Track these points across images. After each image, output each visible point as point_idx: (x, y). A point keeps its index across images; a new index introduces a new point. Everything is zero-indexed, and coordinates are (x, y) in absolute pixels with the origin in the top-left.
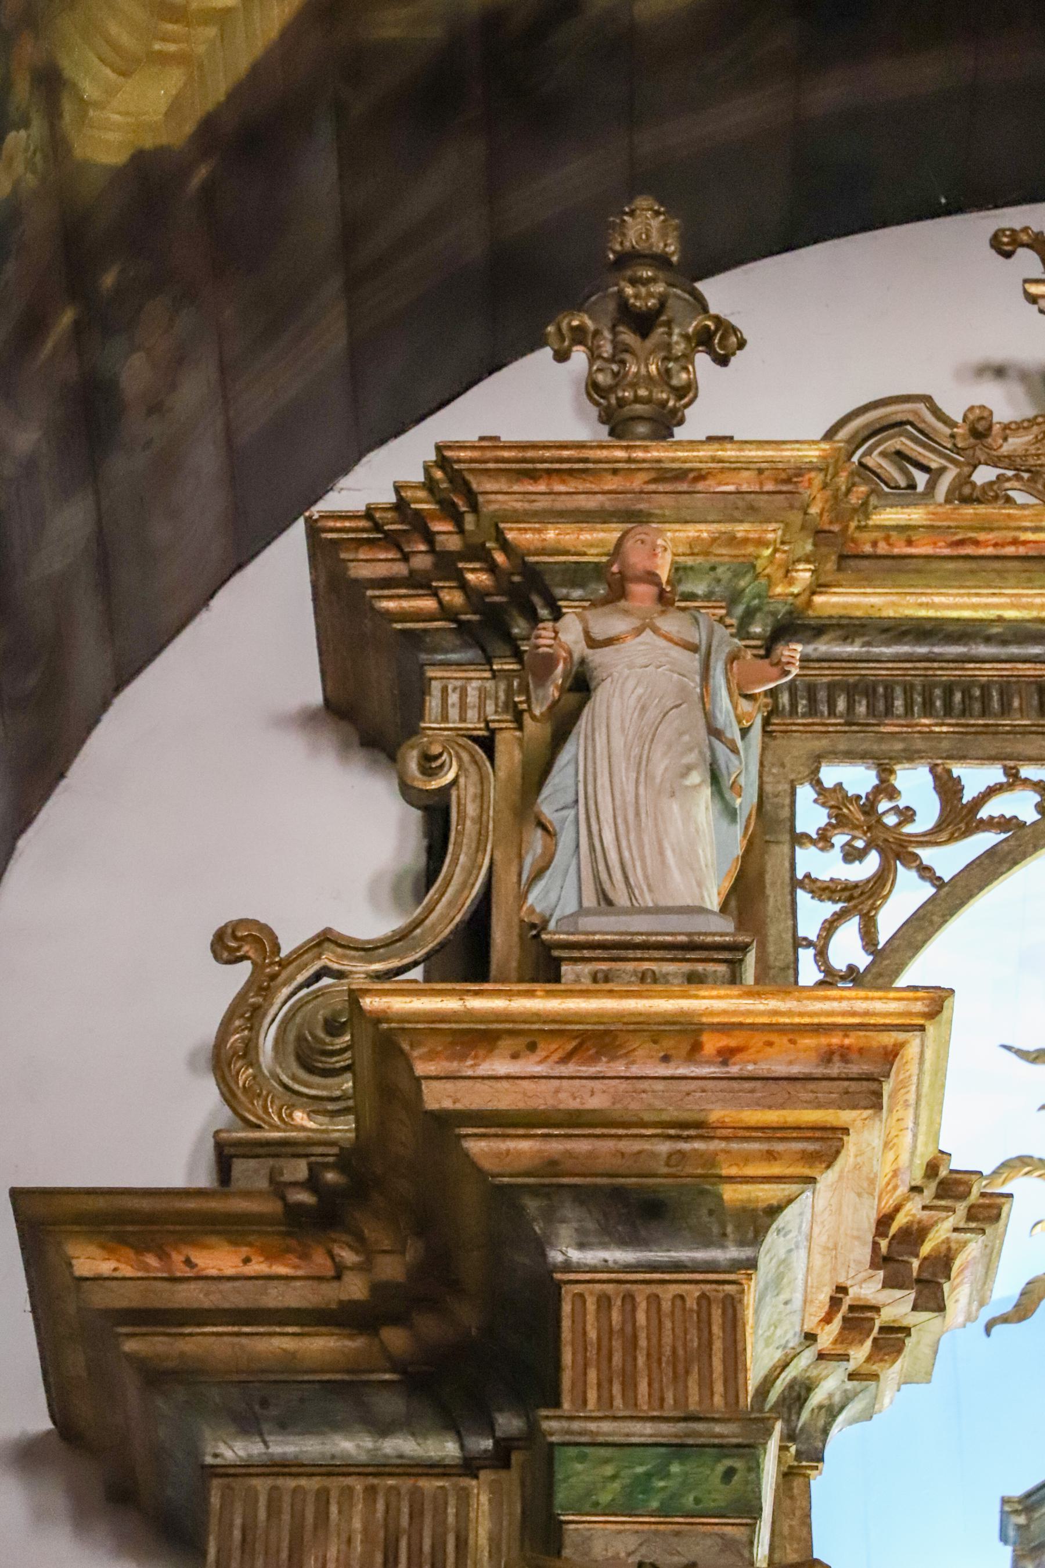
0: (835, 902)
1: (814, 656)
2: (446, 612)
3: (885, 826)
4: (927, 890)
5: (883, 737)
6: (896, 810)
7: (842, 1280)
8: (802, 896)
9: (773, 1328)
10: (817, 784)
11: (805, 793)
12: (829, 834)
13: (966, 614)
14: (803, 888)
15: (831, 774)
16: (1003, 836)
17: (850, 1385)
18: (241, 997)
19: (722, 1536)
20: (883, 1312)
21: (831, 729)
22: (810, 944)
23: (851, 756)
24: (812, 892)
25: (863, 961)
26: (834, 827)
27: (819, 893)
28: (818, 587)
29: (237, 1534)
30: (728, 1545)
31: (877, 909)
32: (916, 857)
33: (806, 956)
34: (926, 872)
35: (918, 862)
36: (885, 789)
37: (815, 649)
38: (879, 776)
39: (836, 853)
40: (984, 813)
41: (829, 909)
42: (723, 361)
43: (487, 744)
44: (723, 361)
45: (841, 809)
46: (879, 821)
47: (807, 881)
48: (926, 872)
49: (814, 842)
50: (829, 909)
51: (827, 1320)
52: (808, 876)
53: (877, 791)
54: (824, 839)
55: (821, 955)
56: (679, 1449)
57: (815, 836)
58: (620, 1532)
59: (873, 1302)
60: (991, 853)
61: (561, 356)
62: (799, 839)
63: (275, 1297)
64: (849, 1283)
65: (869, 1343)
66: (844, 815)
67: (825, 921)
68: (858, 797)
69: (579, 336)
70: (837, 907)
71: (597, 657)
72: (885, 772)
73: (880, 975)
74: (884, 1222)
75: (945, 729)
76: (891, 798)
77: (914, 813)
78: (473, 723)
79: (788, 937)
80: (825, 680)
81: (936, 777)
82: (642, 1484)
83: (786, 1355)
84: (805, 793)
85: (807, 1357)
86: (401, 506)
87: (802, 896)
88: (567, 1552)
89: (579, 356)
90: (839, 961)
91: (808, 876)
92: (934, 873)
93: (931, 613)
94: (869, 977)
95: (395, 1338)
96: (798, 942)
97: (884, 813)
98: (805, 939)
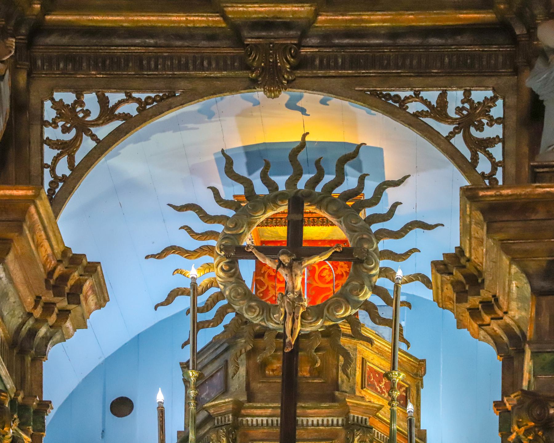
0: (58, 149)
3: (78, 117)
4: (94, 144)
8: (46, 147)
10: (52, 99)
11: (48, 104)
12: (57, 121)
14: (46, 144)
15: (57, 96)
22: (48, 166)
24: (48, 145)
25: (68, 173)
26: (59, 118)
27: (52, 145)
31: (75, 152)
32: (90, 130)
33: (47, 171)
34: (93, 137)
35: (90, 133)
36: (79, 102)
38: (77, 96)
39: (60, 129)
41: (56, 152)
45: (61, 111)
46: (76, 116)
47: (48, 141)
48: (93, 137)
49: (50, 124)
50: (56, 152)
52: (48, 138)
53: (76, 102)
54: (54, 124)
57: (51, 122)
66: (63, 113)
67: (54, 157)
68: (68, 105)
70: (59, 152)
72: (79, 95)
76: (81, 106)
77: (90, 113)
79: (39, 163)
84: (48, 104)
87: (46, 147)
91: (48, 138)
92: (97, 137)
96: (44, 166)
97: (78, 112)
98: (46, 164)
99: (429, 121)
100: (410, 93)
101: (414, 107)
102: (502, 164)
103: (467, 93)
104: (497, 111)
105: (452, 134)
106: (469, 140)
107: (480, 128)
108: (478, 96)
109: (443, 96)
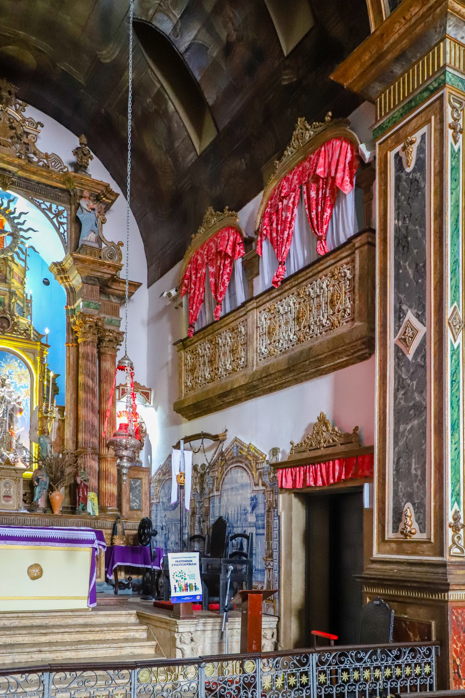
99: (47, 211)
100: (42, 202)
101: (43, 206)
102: (67, 231)
103: (57, 207)
104: (65, 214)
105: (53, 218)
106: (57, 220)
107: (61, 218)
108: (61, 208)
109: (51, 205)
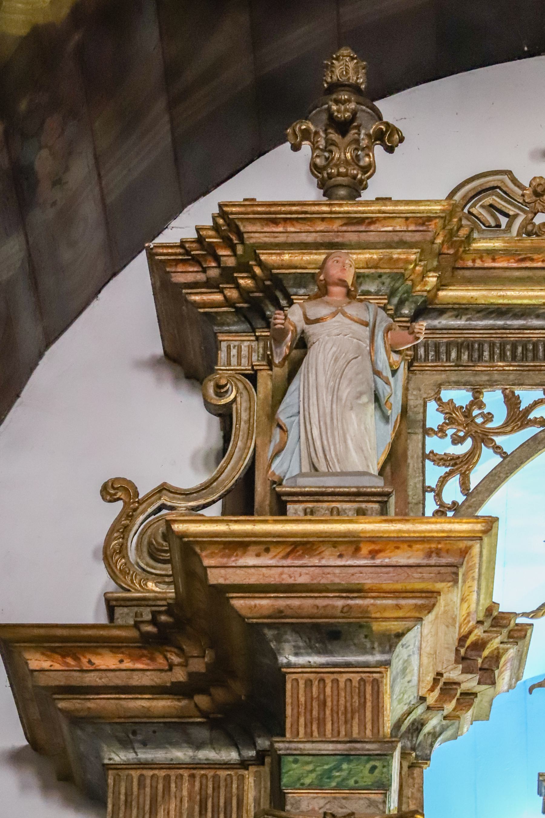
0: (447, 466)
1: (439, 326)
2: (228, 302)
3: (476, 423)
4: (498, 459)
5: (476, 373)
6: (482, 415)
7: (439, 669)
8: (428, 463)
9: (402, 695)
10: (438, 400)
11: (432, 406)
12: (445, 428)
13: (526, 301)
14: (429, 459)
15: (446, 395)
16: (542, 429)
17: (444, 722)
18: (118, 520)
19: (369, 799)
20: (462, 686)
21: (447, 369)
22: (432, 490)
23: (458, 384)
24: (433, 461)
25: (460, 499)
26: (447, 424)
27: (438, 461)
28: (441, 285)
29: (123, 797)
30: (372, 803)
31: (470, 470)
32: (493, 440)
33: (430, 497)
34: (497, 449)
35: (493, 444)
36: (477, 402)
37: (439, 323)
38: (473, 395)
39: (448, 439)
40: (531, 416)
41: (443, 470)
42: (390, 150)
43: (253, 378)
44: (390, 150)
45: (452, 414)
46: (473, 421)
47: (431, 455)
48: (497, 449)
49: (436, 433)
50: (443, 470)
51: (432, 690)
52: (432, 452)
53: (472, 404)
54: (441, 431)
55: (438, 495)
56: (347, 757)
57: (436, 430)
58: (314, 798)
59: (457, 680)
60: (534, 438)
61: (296, 148)
62: (427, 432)
63: (137, 680)
64: (443, 671)
65: (454, 701)
66: (453, 418)
67: (441, 477)
68: (462, 407)
69: (306, 135)
70: (448, 469)
71: (311, 329)
72: (477, 392)
73: (470, 507)
74: (462, 639)
75: (511, 368)
76: (480, 408)
77: (493, 416)
78: (245, 366)
79: (420, 486)
80: (445, 340)
81: (505, 396)
82: (329, 774)
83: (410, 708)
84: (432, 406)
85: (420, 709)
86: (200, 240)
87: (428, 463)
88: (288, 807)
89: (306, 147)
90: (447, 499)
91: (432, 452)
92: (503, 450)
93: (506, 301)
94: (464, 508)
95: (202, 700)
96: (425, 489)
97: (476, 416)
98: (429, 487)
